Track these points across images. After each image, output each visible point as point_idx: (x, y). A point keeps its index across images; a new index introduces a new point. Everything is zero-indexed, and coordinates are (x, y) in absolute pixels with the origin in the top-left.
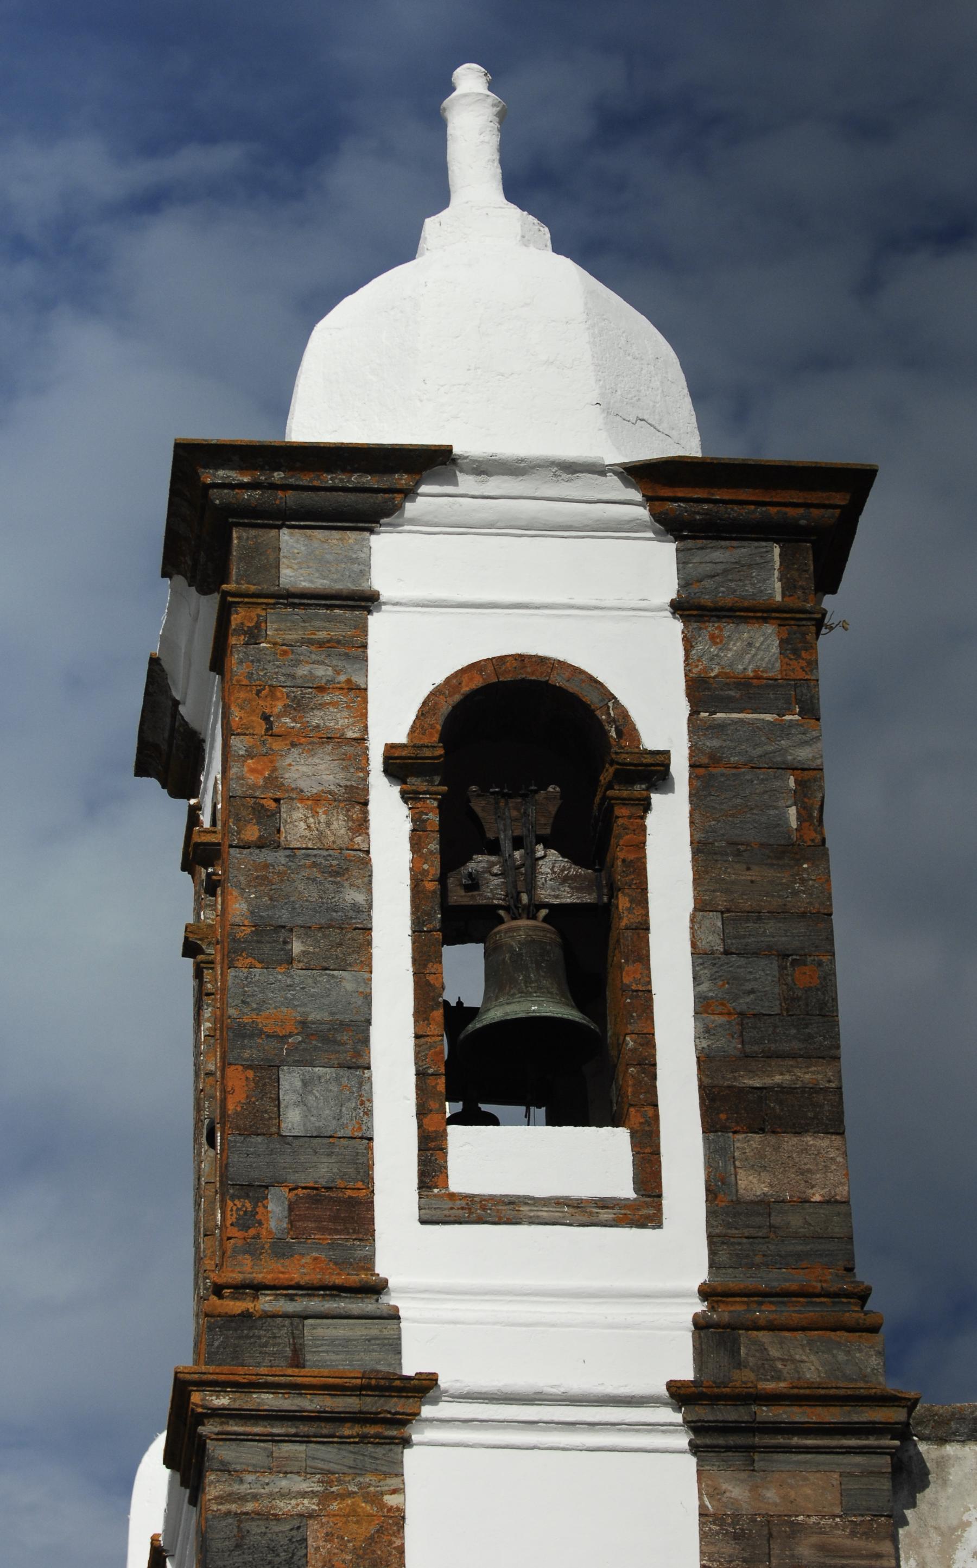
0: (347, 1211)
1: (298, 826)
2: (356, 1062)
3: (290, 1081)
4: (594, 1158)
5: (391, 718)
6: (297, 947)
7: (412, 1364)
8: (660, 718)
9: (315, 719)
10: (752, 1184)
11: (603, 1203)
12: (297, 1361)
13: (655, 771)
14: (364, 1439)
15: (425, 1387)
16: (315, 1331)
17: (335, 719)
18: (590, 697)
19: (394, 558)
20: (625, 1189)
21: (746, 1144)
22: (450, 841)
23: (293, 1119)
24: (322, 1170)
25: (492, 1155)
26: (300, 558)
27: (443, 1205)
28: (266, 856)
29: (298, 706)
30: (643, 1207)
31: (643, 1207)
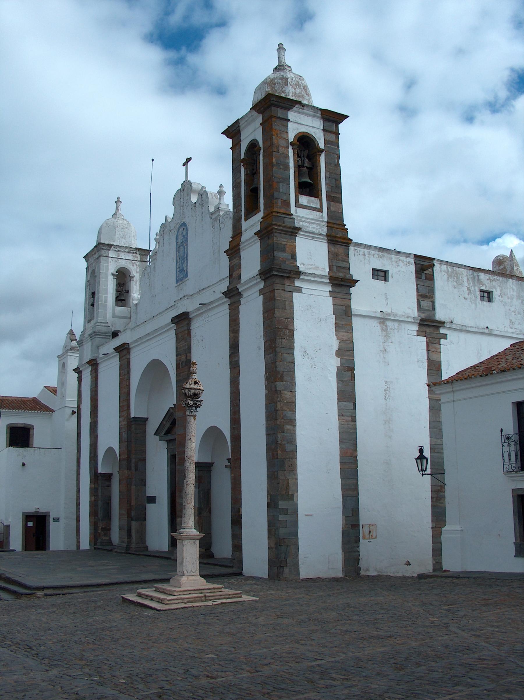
0: (287, 204)
1: (281, 150)
2: (288, 184)
3: (281, 185)
4: (313, 202)
5: (291, 137)
6: (281, 167)
7: (297, 225)
8: (322, 145)
9: (283, 135)
10: (333, 209)
11: (316, 208)
12: (284, 223)
13: (321, 151)
14: (292, 235)
15: (299, 229)
16: (286, 219)
17: (285, 136)
18: (314, 139)
19: (292, 115)
20: (318, 206)
21: (332, 203)
22: (298, 155)
23: (281, 190)
24: (285, 198)
25: (304, 200)
26: (280, 113)
27: (298, 205)
28: (277, 153)
29: (281, 133)
30: (320, 210)
31: (320, 210)
